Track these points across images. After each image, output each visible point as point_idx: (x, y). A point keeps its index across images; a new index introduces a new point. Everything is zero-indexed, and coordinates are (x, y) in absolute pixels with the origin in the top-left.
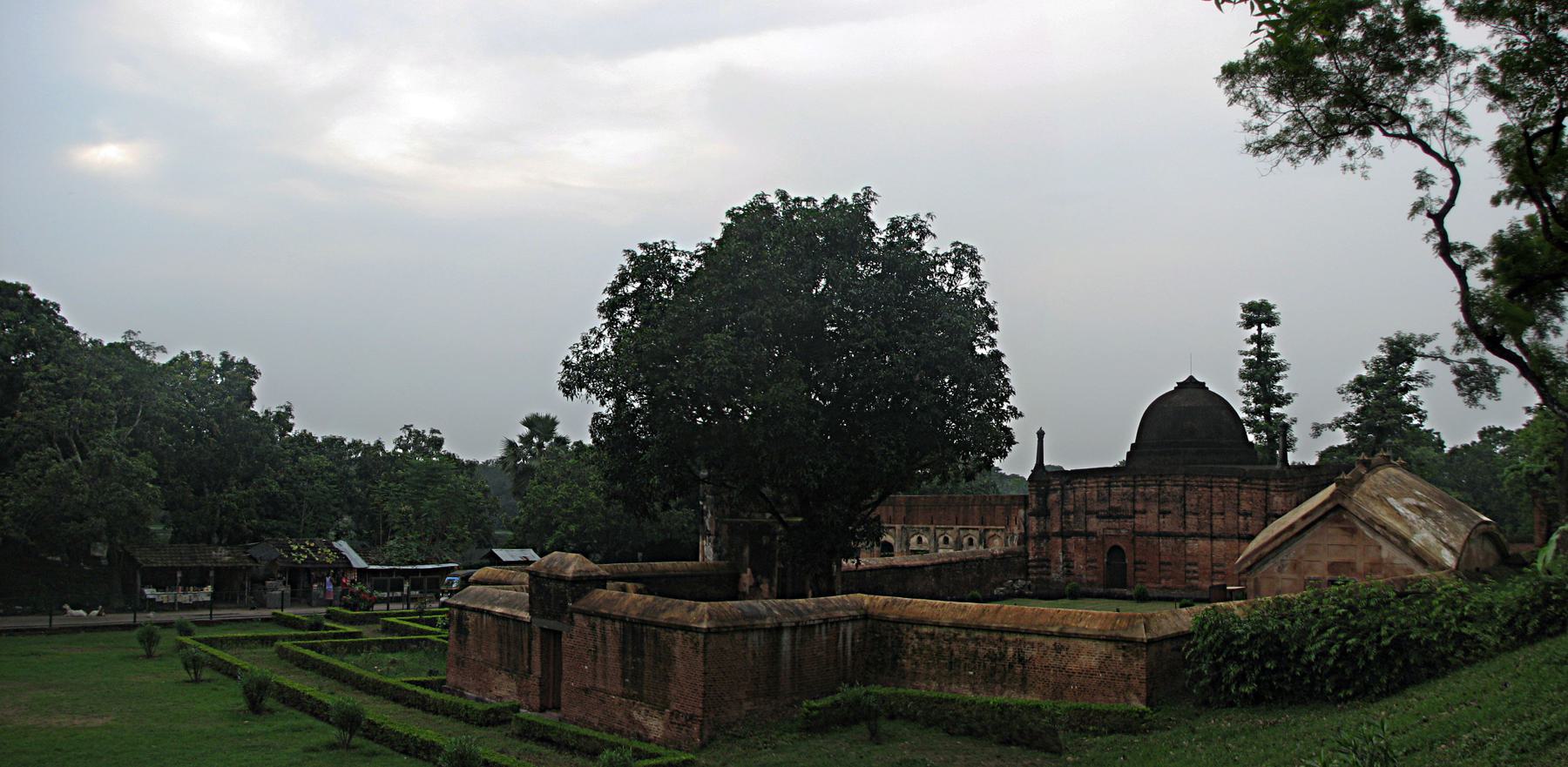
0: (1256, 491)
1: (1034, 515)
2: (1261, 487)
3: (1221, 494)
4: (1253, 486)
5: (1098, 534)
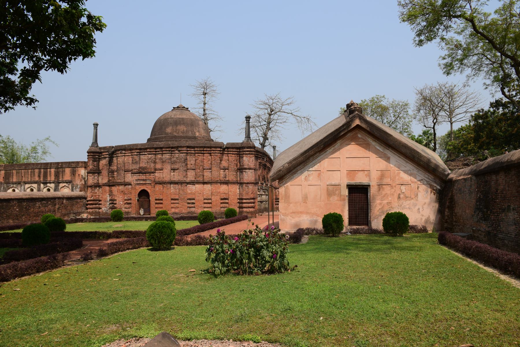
1: (91, 173)
2: (234, 153)
3: (210, 157)
4: (229, 152)
5: (132, 184)
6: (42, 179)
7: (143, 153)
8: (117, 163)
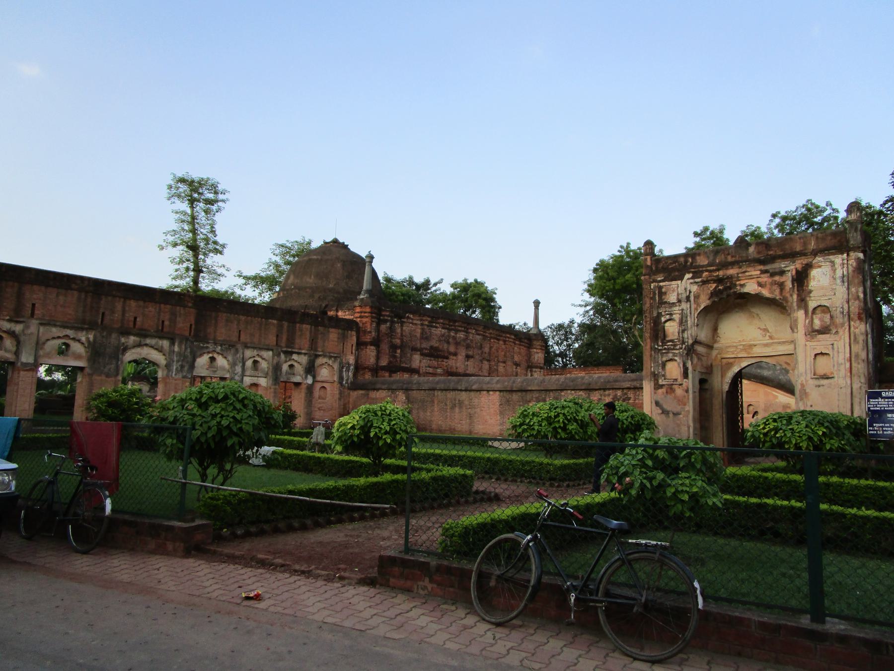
0: (523, 347)
3: (503, 347)
8: (402, 334)
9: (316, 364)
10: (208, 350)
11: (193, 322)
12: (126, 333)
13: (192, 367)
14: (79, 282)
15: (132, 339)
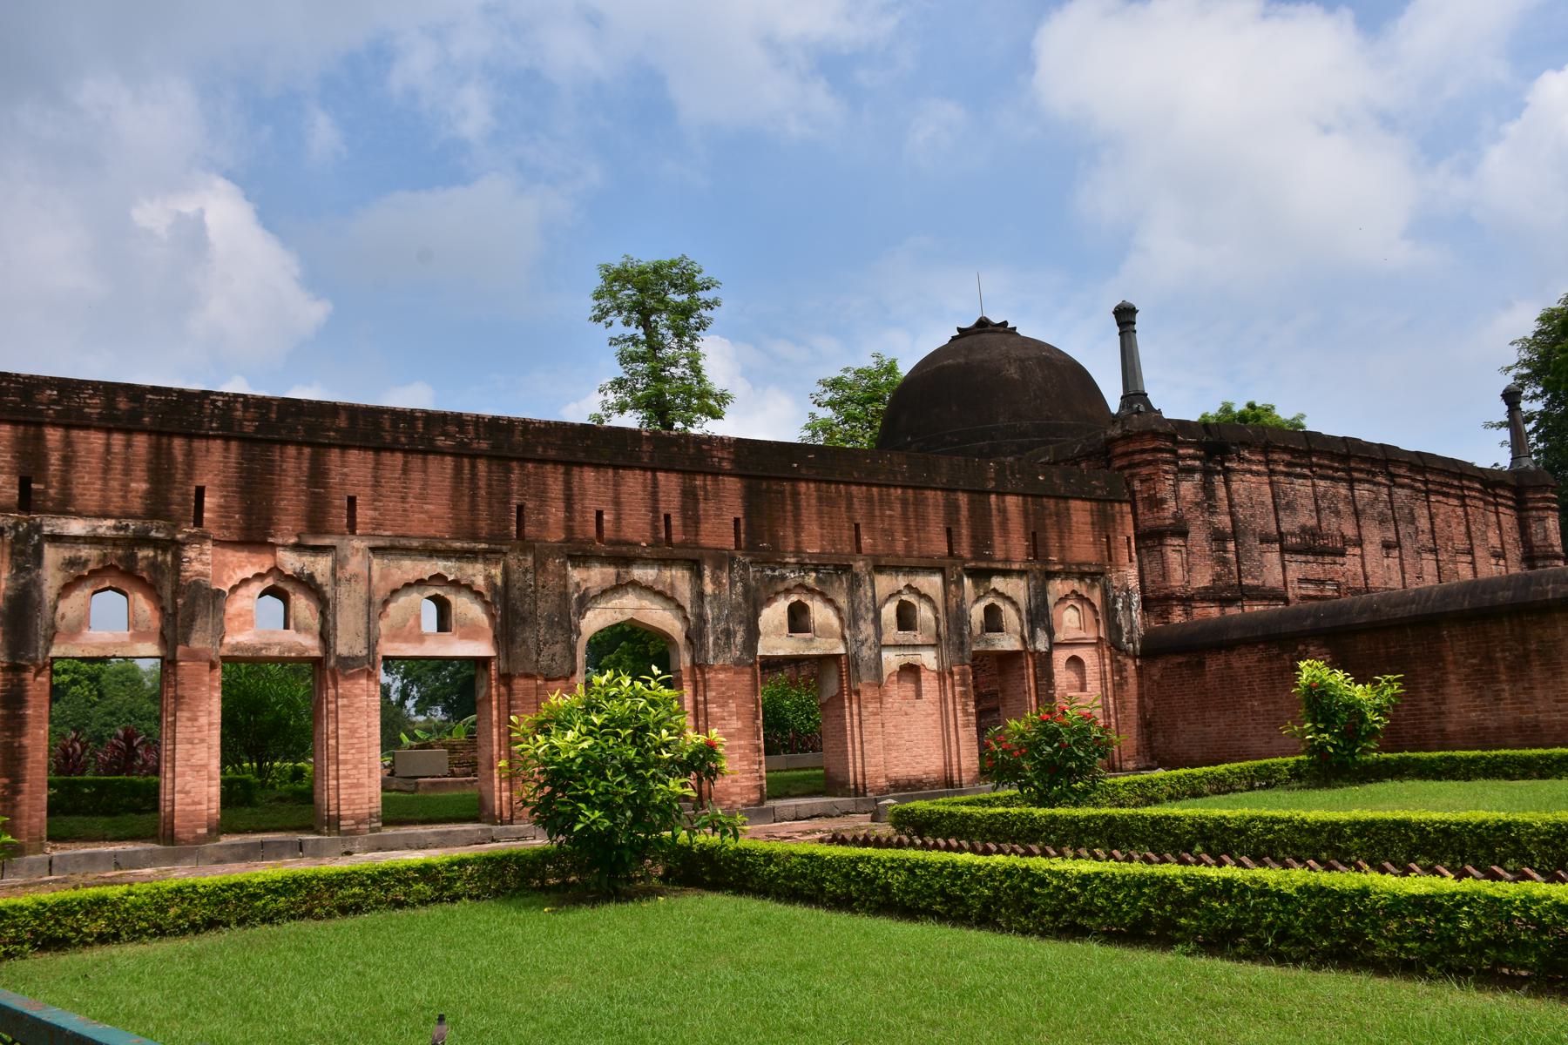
5: (1290, 595)
6: (965, 550)
7: (1299, 470)
9: (1051, 600)
10: (786, 585)
11: (740, 515)
12: (582, 558)
13: (753, 634)
14: (452, 429)
15: (596, 576)
